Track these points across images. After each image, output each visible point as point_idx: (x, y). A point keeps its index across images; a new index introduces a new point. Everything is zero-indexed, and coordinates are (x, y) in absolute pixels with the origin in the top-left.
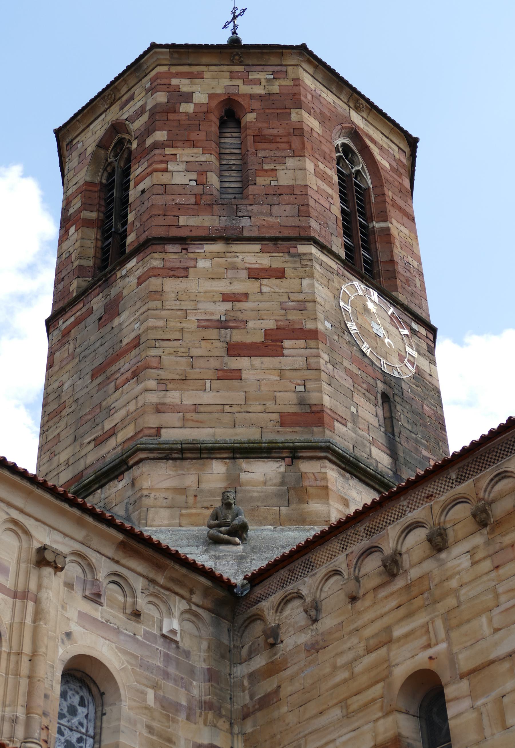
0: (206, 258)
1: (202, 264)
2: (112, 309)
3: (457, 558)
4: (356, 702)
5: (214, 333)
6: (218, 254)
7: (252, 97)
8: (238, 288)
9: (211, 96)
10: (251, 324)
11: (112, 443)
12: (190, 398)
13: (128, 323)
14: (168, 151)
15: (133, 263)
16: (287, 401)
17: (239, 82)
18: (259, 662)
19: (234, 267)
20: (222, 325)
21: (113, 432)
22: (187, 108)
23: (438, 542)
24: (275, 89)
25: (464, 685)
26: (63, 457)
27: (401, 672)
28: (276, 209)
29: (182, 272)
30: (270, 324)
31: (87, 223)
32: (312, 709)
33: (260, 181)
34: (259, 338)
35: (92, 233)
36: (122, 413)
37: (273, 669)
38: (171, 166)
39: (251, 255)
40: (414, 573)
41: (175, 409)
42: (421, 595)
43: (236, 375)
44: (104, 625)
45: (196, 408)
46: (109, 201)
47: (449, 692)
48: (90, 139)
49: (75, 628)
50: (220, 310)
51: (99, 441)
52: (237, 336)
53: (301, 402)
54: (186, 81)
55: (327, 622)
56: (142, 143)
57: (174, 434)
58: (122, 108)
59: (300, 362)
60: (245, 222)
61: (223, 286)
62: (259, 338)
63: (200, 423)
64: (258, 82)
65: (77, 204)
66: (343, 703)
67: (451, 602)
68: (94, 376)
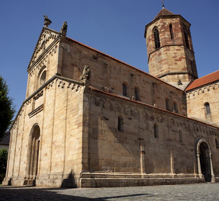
1: (171, 49)
2: (160, 54)
3: (210, 92)
4: (199, 104)
5: (173, 58)
6: (173, 47)
7: (174, 23)
8: (176, 52)
9: (169, 23)
10: (178, 57)
11: (163, 72)
12: (172, 67)
13: (163, 56)
14: (165, 32)
15: (162, 48)
17: (172, 21)
20: (174, 57)
21: (163, 70)
22: (166, 25)
23: (209, 90)
24: (176, 22)
25: (211, 104)
26: (156, 72)
27: (204, 102)
28: (179, 41)
29: (169, 50)
30: (180, 57)
31: (153, 40)
32: (194, 104)
33: (176, 36)
34: (178, 59)
38: (165, 35)
39: (176, 47)
40: (206, 93)
41: (171, 68)
45: (173, 68)
46: (155, 37)
47: (210, 104)
48: (151, 27)
50: (174, 55)
51: (161, 71)
52: (176, 59)
54: (165, 21)
56: (160, 31)
57: (171, 71)
58: (156, 24)
60: (175, 43)
62: (178, 59)
63: (174, 70)
64: (174, 21)
67: (210, 96)
68: (159, 62)
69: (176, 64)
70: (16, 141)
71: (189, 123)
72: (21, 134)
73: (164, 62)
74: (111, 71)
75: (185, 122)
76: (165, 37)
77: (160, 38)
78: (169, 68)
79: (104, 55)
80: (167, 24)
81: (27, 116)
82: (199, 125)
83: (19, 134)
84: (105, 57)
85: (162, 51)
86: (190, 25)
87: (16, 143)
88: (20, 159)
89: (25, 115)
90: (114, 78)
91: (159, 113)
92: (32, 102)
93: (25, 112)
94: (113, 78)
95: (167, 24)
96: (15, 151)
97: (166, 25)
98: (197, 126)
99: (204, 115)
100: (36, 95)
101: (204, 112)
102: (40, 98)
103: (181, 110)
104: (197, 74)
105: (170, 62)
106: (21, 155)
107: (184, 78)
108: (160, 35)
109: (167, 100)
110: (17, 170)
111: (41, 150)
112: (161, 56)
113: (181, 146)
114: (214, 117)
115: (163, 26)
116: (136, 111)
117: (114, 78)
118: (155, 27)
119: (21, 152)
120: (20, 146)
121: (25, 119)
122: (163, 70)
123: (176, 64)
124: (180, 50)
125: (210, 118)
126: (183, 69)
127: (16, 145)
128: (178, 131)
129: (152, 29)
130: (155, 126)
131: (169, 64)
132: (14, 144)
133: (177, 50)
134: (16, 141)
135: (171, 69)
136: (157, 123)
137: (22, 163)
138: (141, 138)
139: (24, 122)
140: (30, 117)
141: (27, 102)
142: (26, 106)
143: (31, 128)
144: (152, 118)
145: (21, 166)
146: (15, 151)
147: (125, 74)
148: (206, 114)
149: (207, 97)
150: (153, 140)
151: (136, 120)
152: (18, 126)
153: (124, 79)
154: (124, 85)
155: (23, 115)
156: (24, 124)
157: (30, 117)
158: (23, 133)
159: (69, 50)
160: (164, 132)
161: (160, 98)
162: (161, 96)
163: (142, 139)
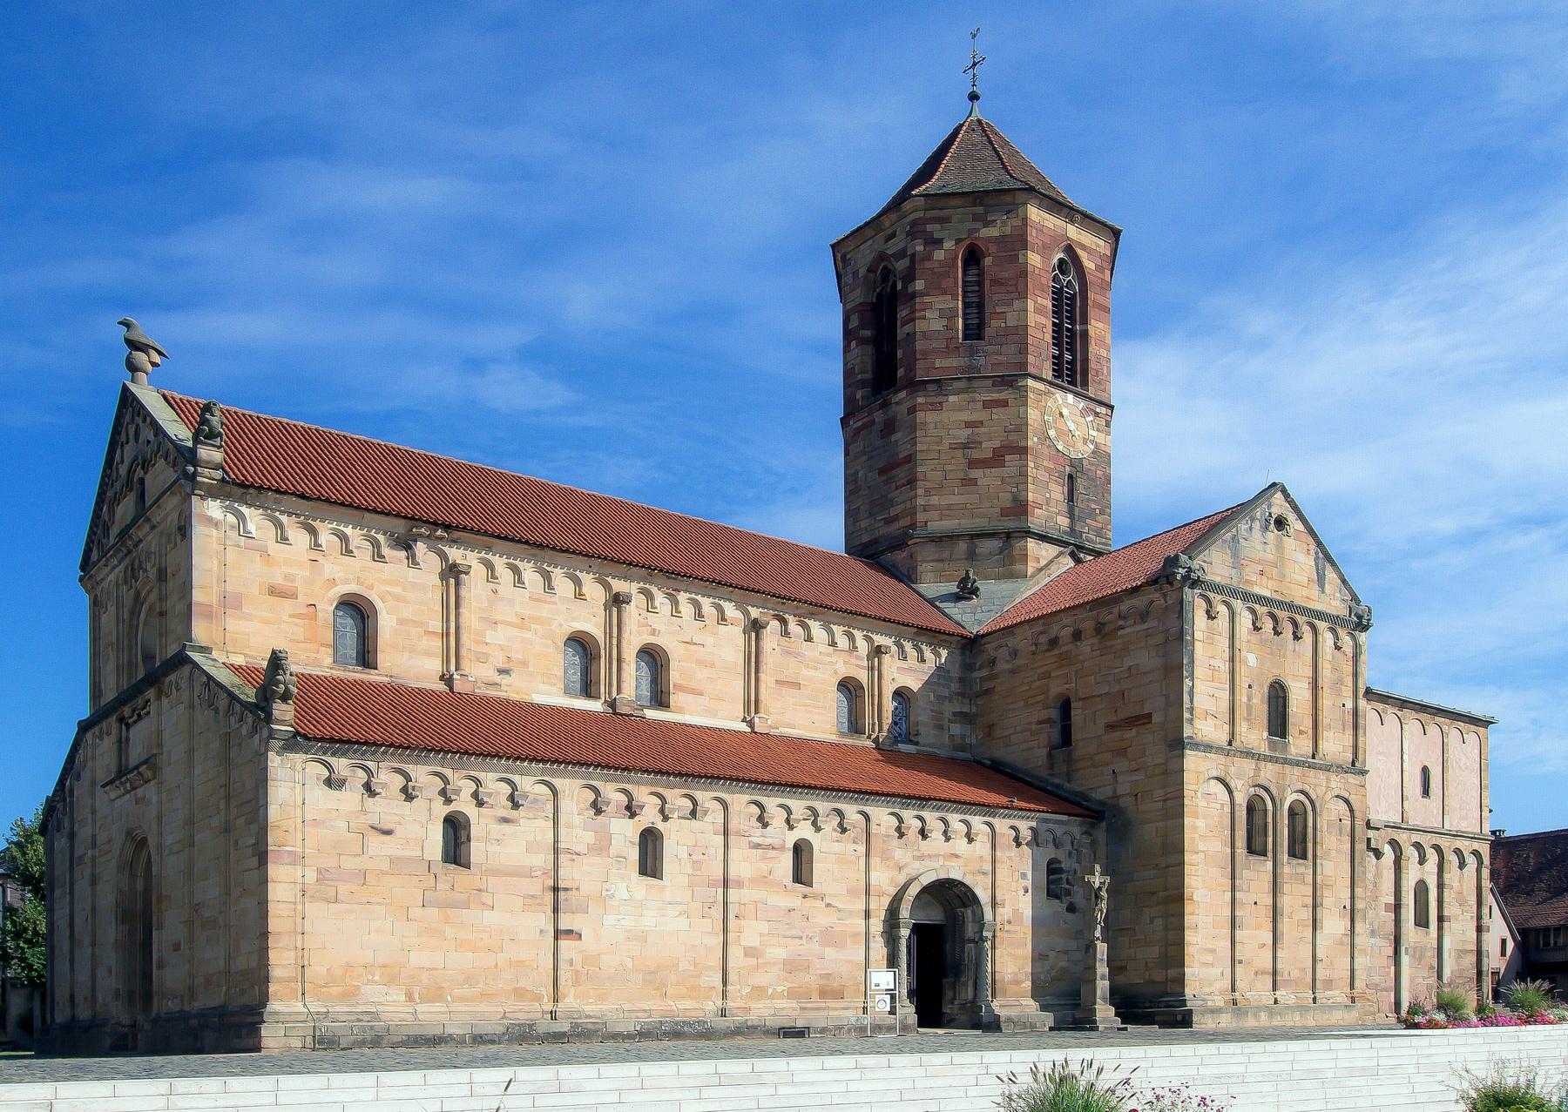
16: (1005, 499)
21: (896, 518)
35: (869, 349)
36: (902, 507)
43: (974, 482)
44: (910, 669)
45: (949, 507)
49: (896, 675)
53: (1015, 499)
55: (1020, 661)
63: (951, 517)
65: (855, 322)
67: (1079, 666)
69: (969, 482)
73: (901, 473)
123: (969, 482)
126: (1004, 513)
129: (862, 272)
131: (928, 485)
135: (933, 514)
161: (797, 686)
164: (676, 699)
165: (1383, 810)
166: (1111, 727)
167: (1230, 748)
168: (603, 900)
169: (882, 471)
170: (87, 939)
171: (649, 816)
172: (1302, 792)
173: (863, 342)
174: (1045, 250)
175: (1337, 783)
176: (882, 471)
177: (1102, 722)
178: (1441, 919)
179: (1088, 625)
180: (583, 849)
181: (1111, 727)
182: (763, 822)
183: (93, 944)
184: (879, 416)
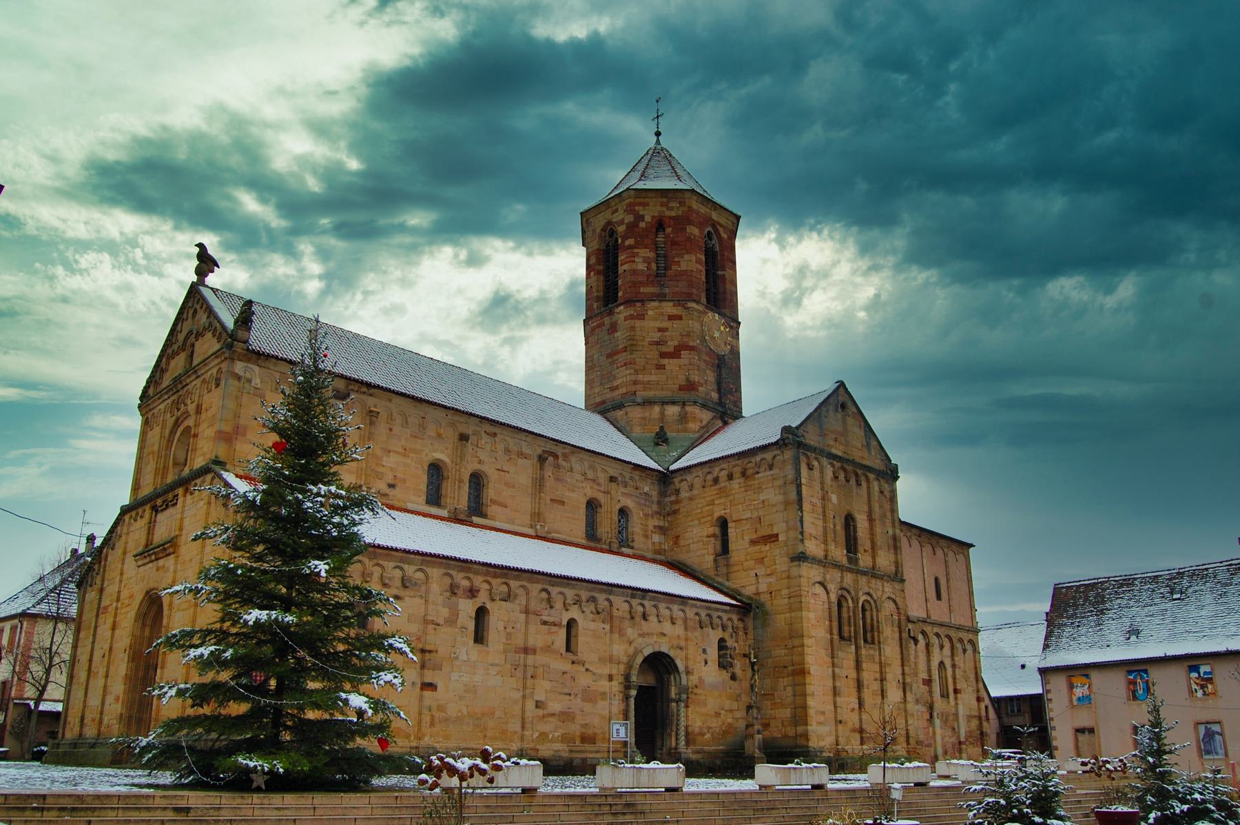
0: (652, 308)
1: (650, 313)
2: (613, 328)
6: (657, 308)
7: (670, 218)
11: (617, 393)
15: (622, 308)
16: (682, 380)
18: (673, 498)
19: (662, 314)
20: (658, 343)
21: (617, 388)
22: (642, 225)
23: (730, 477)
26: (597, 390)
27: (716, 515)
29: (641, 317)
33: (674, 268)
34: (671, 350)
35: (601, 278)
36: (619, 381)
37: (677, 502)
39: (669, 308)
42: (723, 492)
45: (648, 383)
48: (599, 222)
50: (656, 336)
51: (613, 389)
52: (664, 349)
53: (687, 380)
55: (695, 492)
56: (623, 242)
59: (687, 361)
60: (667, 290)
61: (658, 324)
62: (671, 350)
64: (672, 209)
65: (593, 260)
66: (699, 519)
69: (661, 367)
70: (96, 627)
71: (611, 597)
72: (111, 610)
74: (391, 430)
75: (595, 594)
76: (634, 266)
77: (621, 269)
78: (635, 383)
79: (369, 385)
80: (648, 218)
81: (130, 563)
82: (653, 599)
83: (106, 608)
84: (373, 391)
85: (622, 317)
86: (738, 218)
87: (94, 635)
88: (105, 686)
89: (125, 553)
90: (400, 450)
91: (495, 576)
92: (147, 515)
93: (126, 543)
94: (395, 452)
95: (648, 218)
96: (91, 660)
97: (642, 225)
98: (643, 605)
99: (712, 558)
100: (159, 502)
101: (711, 549)
102: (171, 511)
103: (646, 536)
104: (738, 403)
105: (640, 361)
106: (107, 676)
107: (683, 418)
108: (622, 257)
109: (592, 506)
110: (93, 720)
111: (162, 668)
112: (616, 335)
113: (567, 667)
114: (735, 568)
115: (632, 227)
116: (420, 575)
117: (400, 450)
118: (609, 223)
119: (108, 667)
120: (107, 647)
121: (126, 566)
122: (617, 388)
123: (661, 367)
124: (680, 318)
125: (724, 570)
126: (681, 388)
127: (93, 643)
128: (565, 623)
129: (598, 230)
130: (481, 613)
132: (87, 637)
133: (672, 318)
134: (96, 627)
135: (639, 387)
136: (488, 606)
137: (110, 699)
138: (428, 648)
139: (122, 574)
140: (140, 563)
141: (134, 513)
142: (130, 524)
143: (139, 597)
144: (472, 593)
145: (106, 707)
146: (91, 660)
147: (439, 435)
148: (717, 555)
149: (723, 500)
150: (467, 650)
151: (417, 600)
152: (103, 581)
153: (435, 451)
154: (436, 470)
155: (119, 551)
156: (121, 581)
157: (140, 563)
158: (117, 609)
159: (257, 382)
160: (509, 630)
161: (562, 503)
162: (574, 495)
163: (430, 652)
164: (492, 510)
165: (916, 611)
166: (753, 542)
167: (825, 562)
168: (453, 659)
169: (609, 356)
170: (102, 672)
171: (482, 598)
172: (868, 594)
173: (598, 273)
174: (701, 226)
175: (888, 589)
176: (609, 356)
177: (747, 538)
178: (956, 691)
179: (737, 470)
180: (441, 621)
181: (753, 542)
182: (550, 603)
183: (107, 676)
184: (607, 320)
